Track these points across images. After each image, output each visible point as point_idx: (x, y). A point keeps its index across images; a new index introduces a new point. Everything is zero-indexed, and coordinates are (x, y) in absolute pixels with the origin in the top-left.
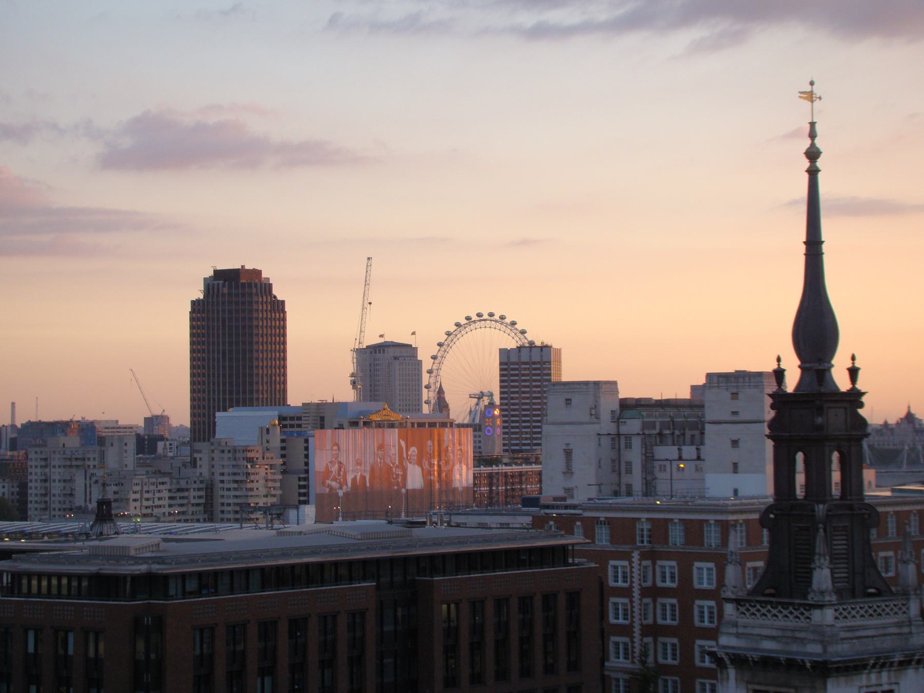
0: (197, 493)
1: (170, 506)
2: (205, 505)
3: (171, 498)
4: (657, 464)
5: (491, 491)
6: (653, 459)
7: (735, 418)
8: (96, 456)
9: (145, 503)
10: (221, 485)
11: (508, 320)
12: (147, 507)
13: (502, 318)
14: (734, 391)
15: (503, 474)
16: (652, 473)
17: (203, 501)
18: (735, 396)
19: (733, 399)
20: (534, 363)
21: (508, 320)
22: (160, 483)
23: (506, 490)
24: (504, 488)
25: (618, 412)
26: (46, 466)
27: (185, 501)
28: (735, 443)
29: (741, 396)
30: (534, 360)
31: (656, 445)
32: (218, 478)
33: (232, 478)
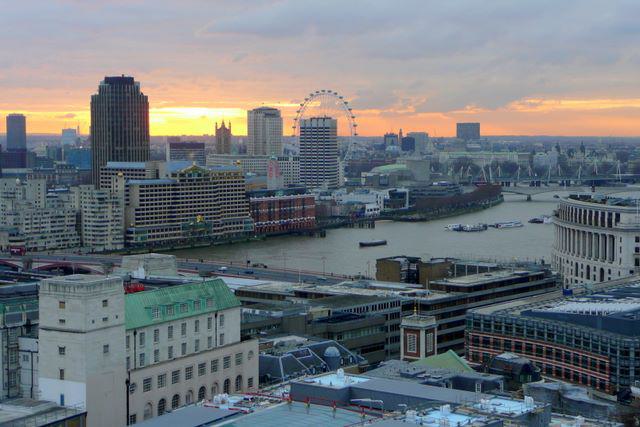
5: (270, 212)
6: (17, 349)
13: (330, 92)
14: (61, 300)
16: (17, 362)
17: (74, 223)
18: (62, 304)
19: (60, 307)
21: (338, 95)
23: (280, 211)
28: (62, 350)
31: (22, 336)
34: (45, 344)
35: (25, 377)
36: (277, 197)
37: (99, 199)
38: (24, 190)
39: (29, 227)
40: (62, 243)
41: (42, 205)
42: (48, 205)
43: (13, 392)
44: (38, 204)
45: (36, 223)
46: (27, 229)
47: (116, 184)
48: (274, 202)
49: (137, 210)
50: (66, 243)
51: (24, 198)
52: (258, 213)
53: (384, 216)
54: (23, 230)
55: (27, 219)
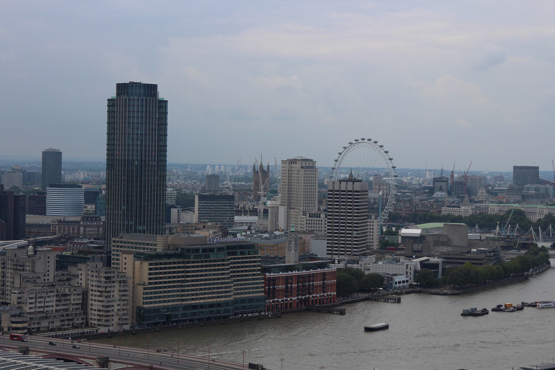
0: (76, 297)
1: (57, 305)
2: (82, 304)
3: (57, 301)
5: (287, 287)
8: (30, 264)
9: (38, 305)
10: (91, 293)
11: (379, 144)
12: (40, 307)
15: (296, 277)
20: (349, 191)
22: (49, 292)
23: (298, 286)
24: (296, 285)
27: (68, 302)
30: (348, 189)
32: (91, 288)
33: (97, 289)
36: (295, 273)
37: (106, 278)
39: (33, 306)
41: (51, 280)
44: (46, 278)
45: (40, 302)
46: (30, 308)
47: (124, 261)
48: (292, 277)
49: (145, 289)
50: (71, 322)
51: (33, 271)
52: (274, 289)
53: (411, 290)
54: (26, 308)
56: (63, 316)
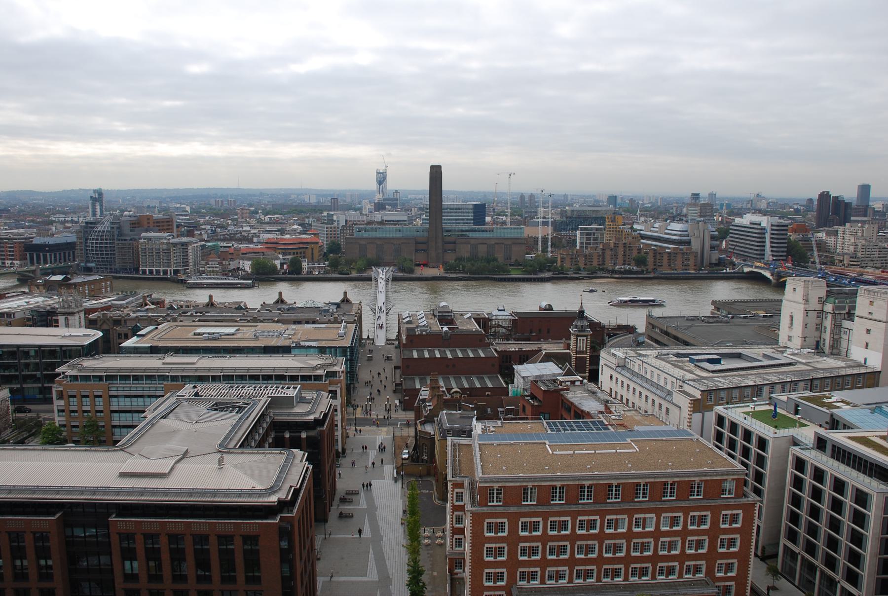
4: (843, 330)
6: (841, 326)
7: (870, 317)
14: (872, 300)
16: (839, 334)
18: (871, 303)
25: (825, 298)
26: (844, 234)
28: (868, 331)
29: (874, 303)
31: (845, 319)
34: (857, 327)
35: (844, 344)
38: (863, 230)
39: (864, 253)
40: (884, 265)
42: (878, 241)
43: (835, 351)
44: (871, 240)
51: (862, 236)
54: (859, 255)
55: (863, 249)
56: (882, 260)
